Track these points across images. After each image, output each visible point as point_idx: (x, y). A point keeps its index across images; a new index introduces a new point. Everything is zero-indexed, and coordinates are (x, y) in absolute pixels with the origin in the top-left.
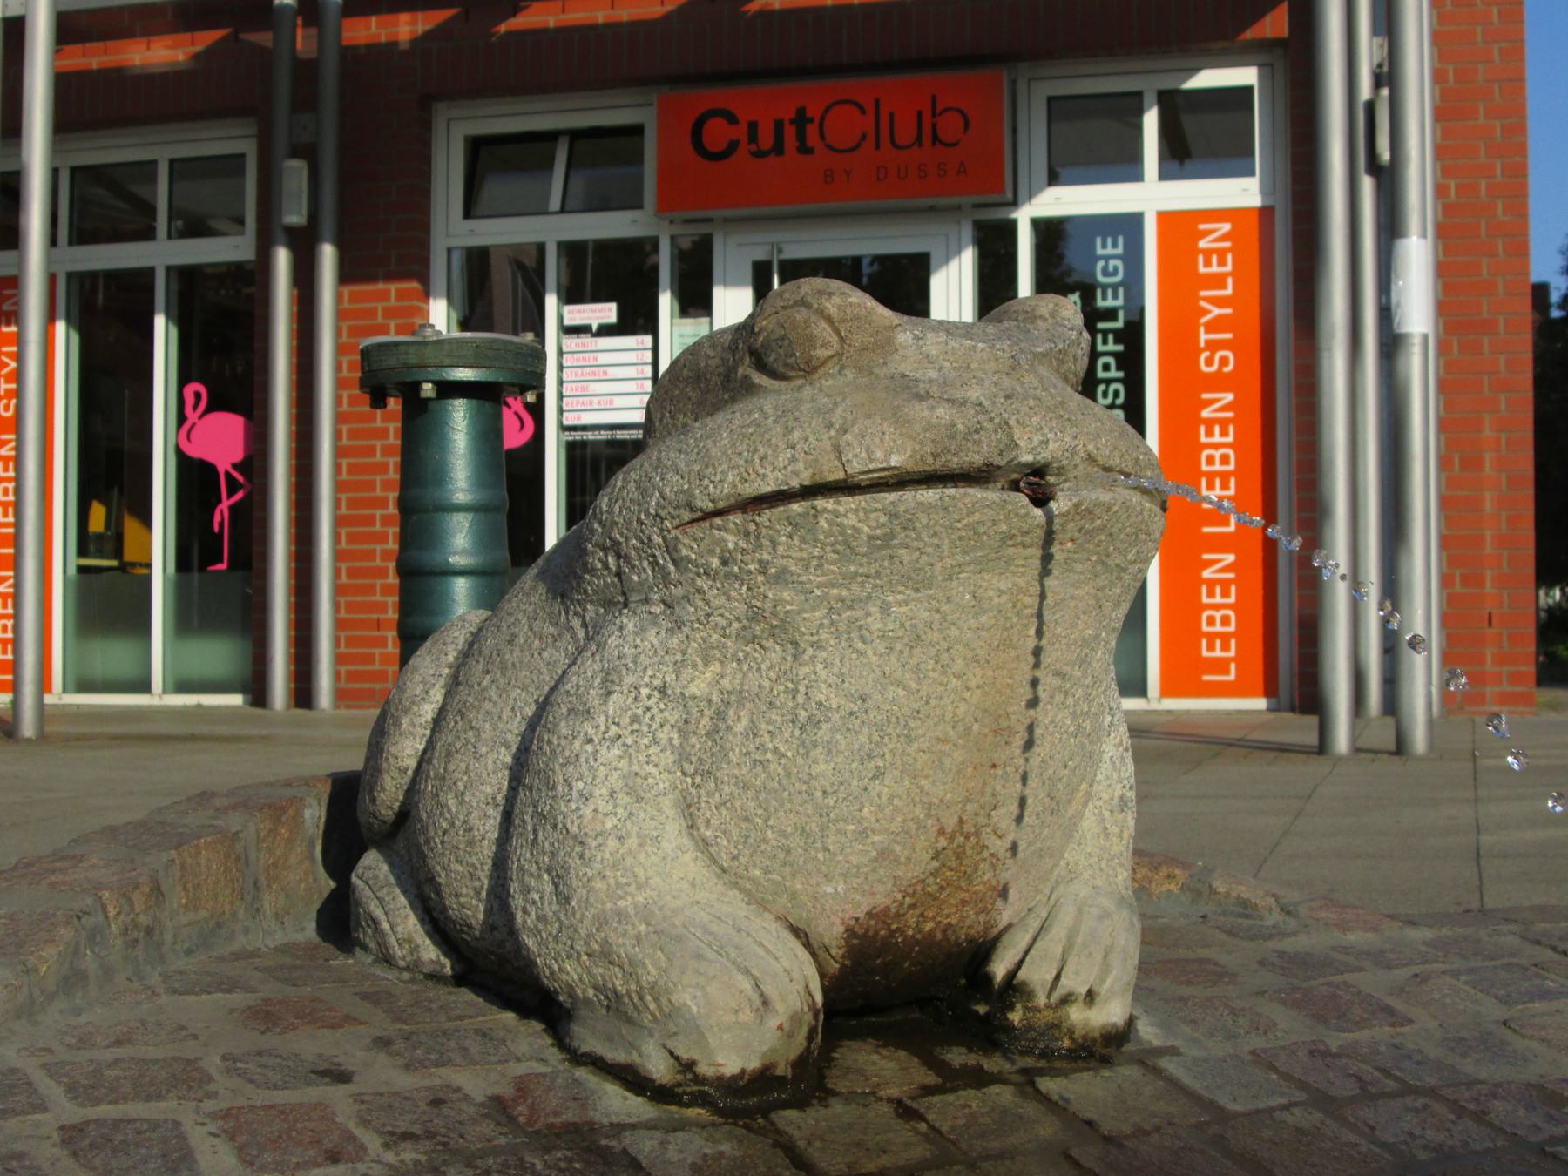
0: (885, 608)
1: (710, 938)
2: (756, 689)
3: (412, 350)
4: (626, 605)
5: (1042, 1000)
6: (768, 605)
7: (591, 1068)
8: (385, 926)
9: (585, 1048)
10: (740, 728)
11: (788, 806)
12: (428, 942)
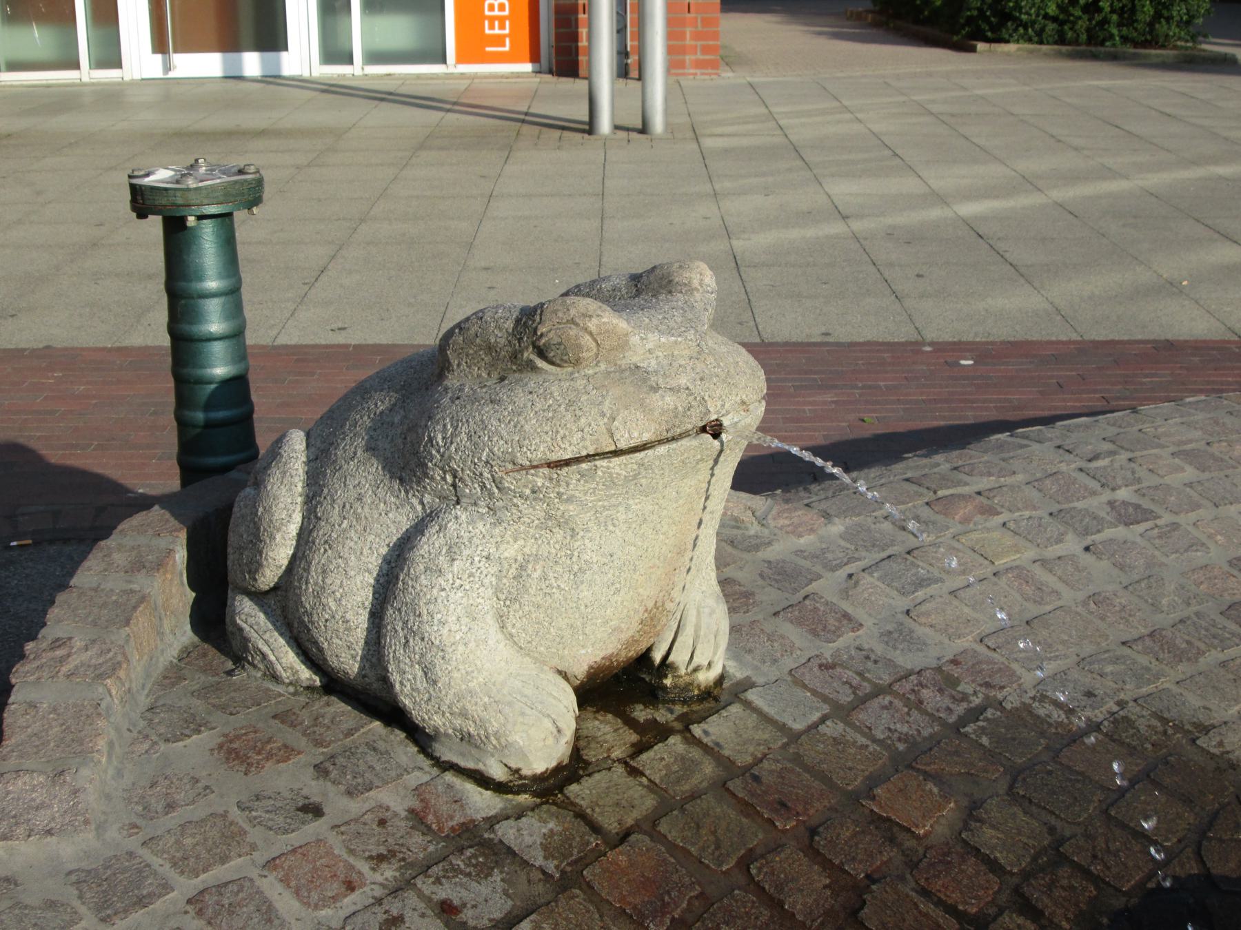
0: (628, 508)
1: (526, 699)
2: (547, 554)
3: (178, 194)
4: (458, 502)
5: (682, 671)
6: (559, 513)
7: (452, 771)
8: (272, 658)
9: (444, 758)
10: (536, 575)
11: (564, 615)
12: (303, 667)
